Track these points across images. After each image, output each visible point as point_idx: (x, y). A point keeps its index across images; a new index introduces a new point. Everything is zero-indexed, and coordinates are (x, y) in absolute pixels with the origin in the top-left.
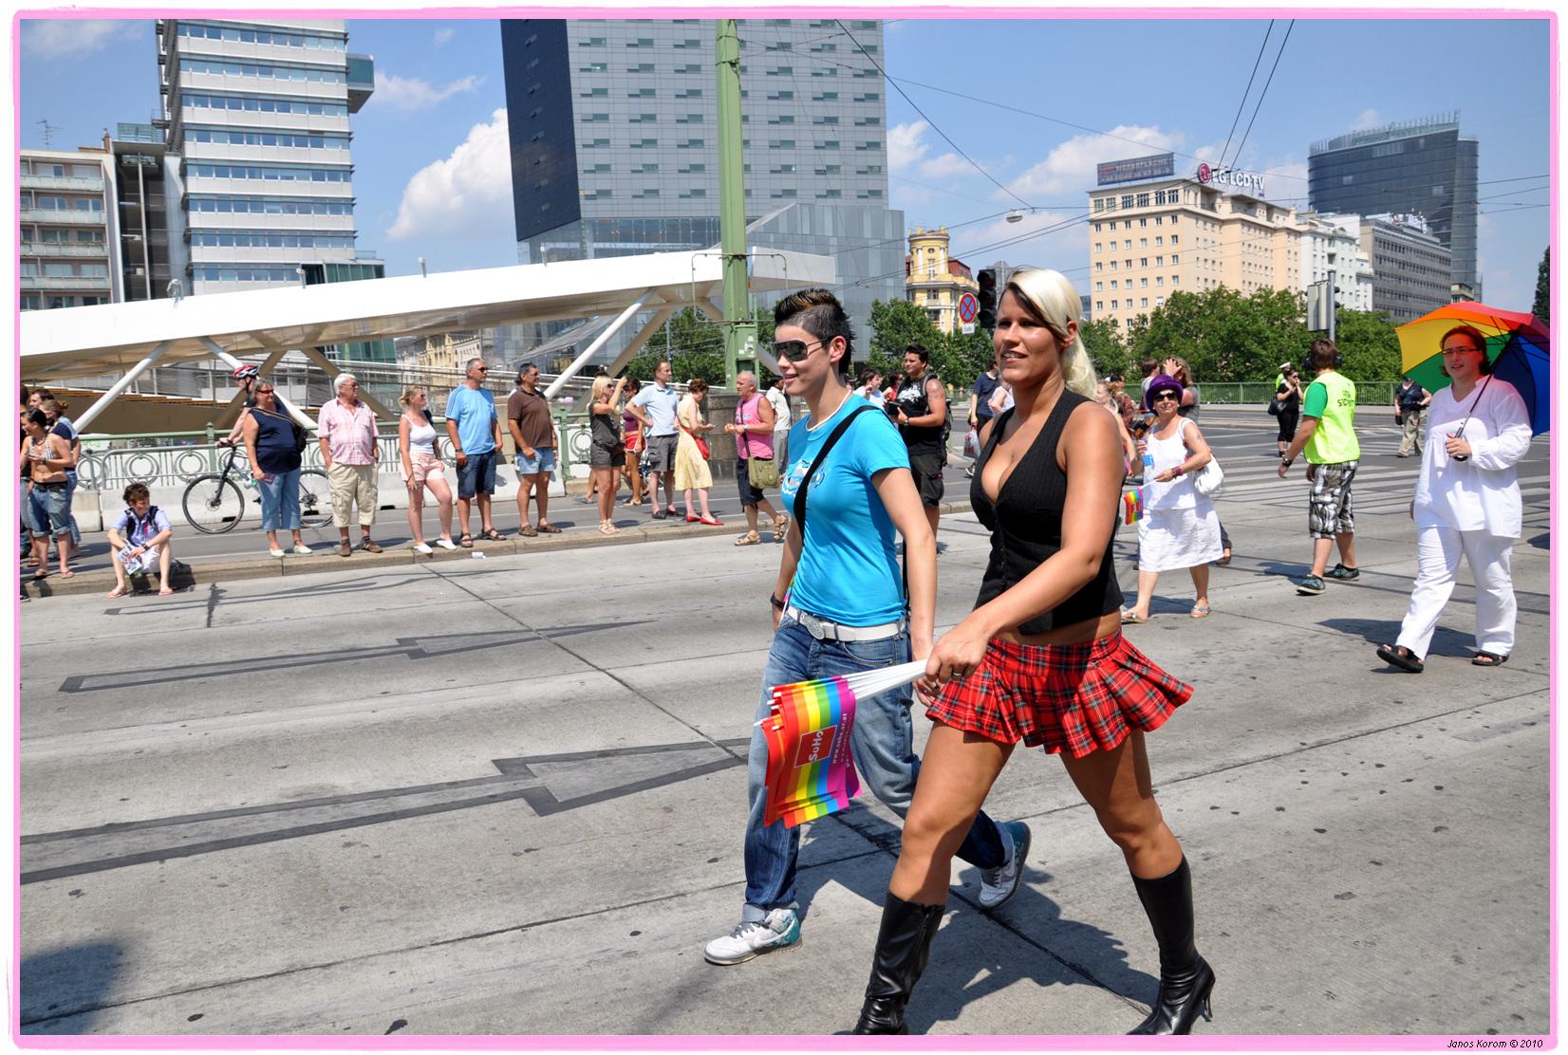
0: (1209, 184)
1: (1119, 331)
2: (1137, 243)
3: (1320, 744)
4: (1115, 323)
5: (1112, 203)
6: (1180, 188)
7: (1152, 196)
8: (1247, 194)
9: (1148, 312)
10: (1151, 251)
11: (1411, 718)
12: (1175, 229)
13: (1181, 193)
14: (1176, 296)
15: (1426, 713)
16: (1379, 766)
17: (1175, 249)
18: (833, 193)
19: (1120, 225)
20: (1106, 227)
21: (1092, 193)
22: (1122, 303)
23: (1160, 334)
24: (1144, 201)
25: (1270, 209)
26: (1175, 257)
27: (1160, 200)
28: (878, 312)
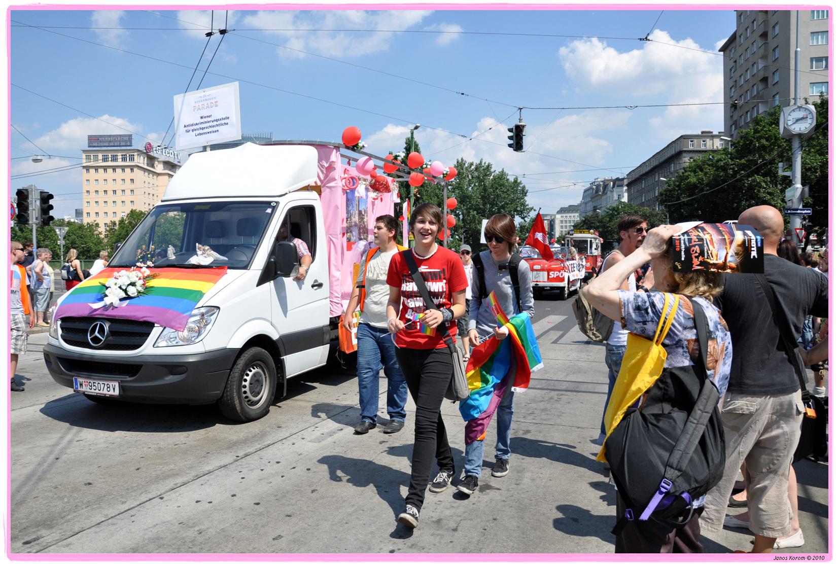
0: (151, 154)
1: (100, 230)
2: (110, 181)
3: (246, 455)
4: (97, 225)
8: (171, 160)
9: (117, 220)
10: (119, 186)
11: (288, 435)
12: (132, 176)
13: (136, 157)
14: (132, 211)
15: (294, 431)
16: (278, 462)
17: (132, 186)
19: (101, 171)
20: (92, 171)
21: (84, 151)
22: (101, 214)
23: (124, 232)
24: (115, 159)
26: (132, 191)
27: (124, 159)
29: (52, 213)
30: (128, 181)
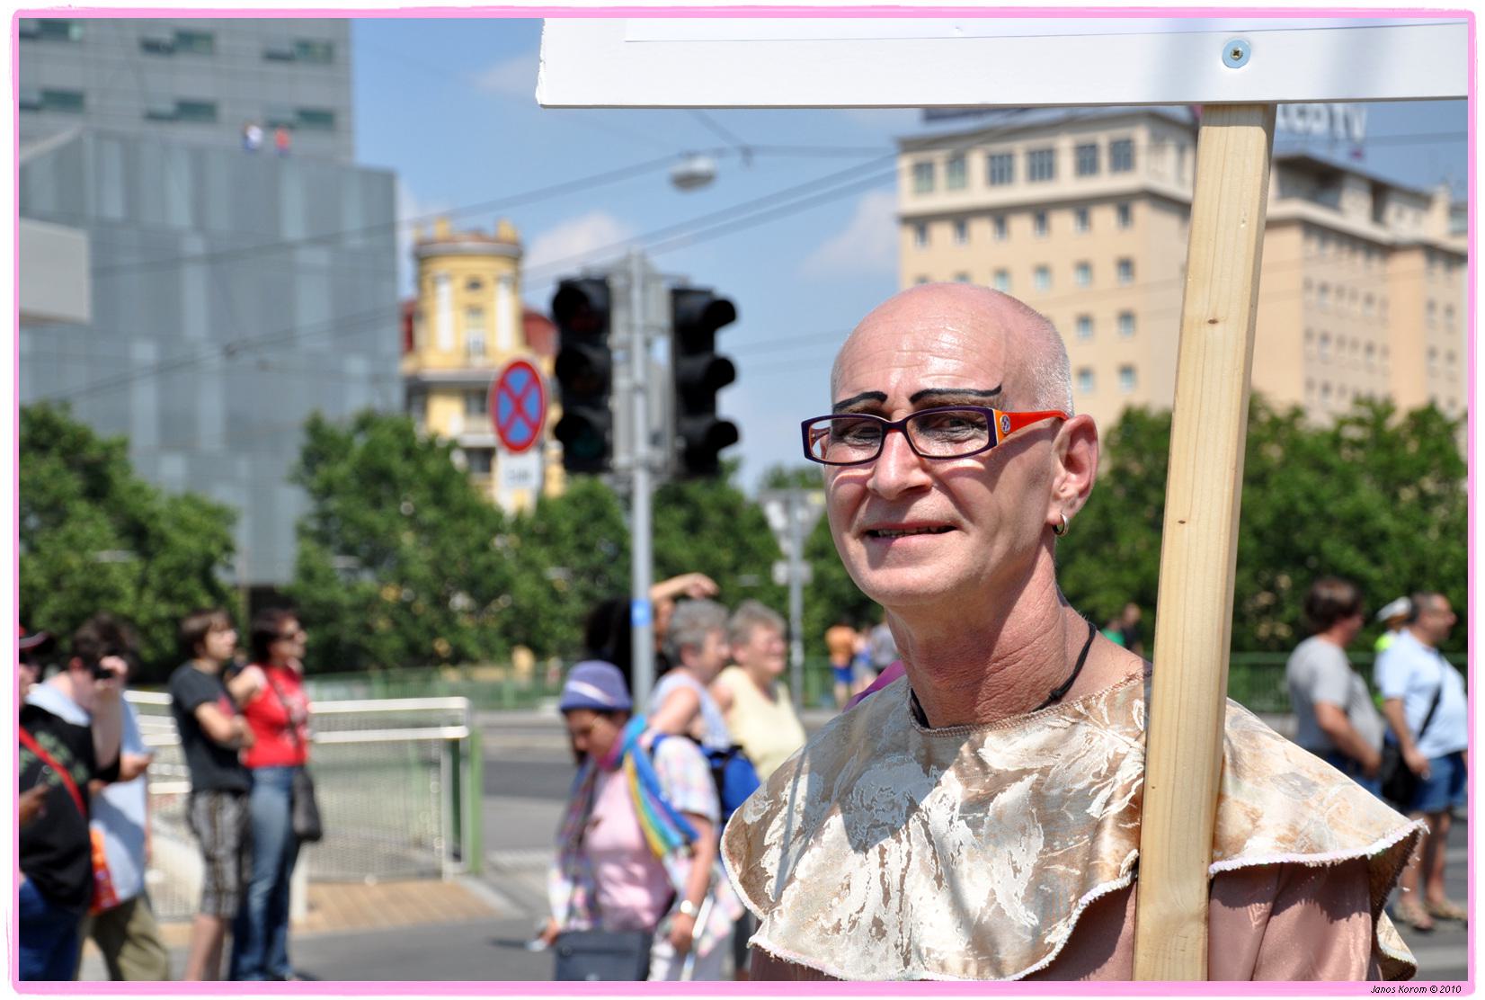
5: (957, 164)
6: (1141, 136)
7: (1066, 162)
8: (1320, 152)
18: (194, 110)
24: (1043, 167)
25: (1380, 192)
26: (1127, 318)
27: (1087, 162)
28: (320, 446)
29: (729, 404)
30: (1106, 273)
